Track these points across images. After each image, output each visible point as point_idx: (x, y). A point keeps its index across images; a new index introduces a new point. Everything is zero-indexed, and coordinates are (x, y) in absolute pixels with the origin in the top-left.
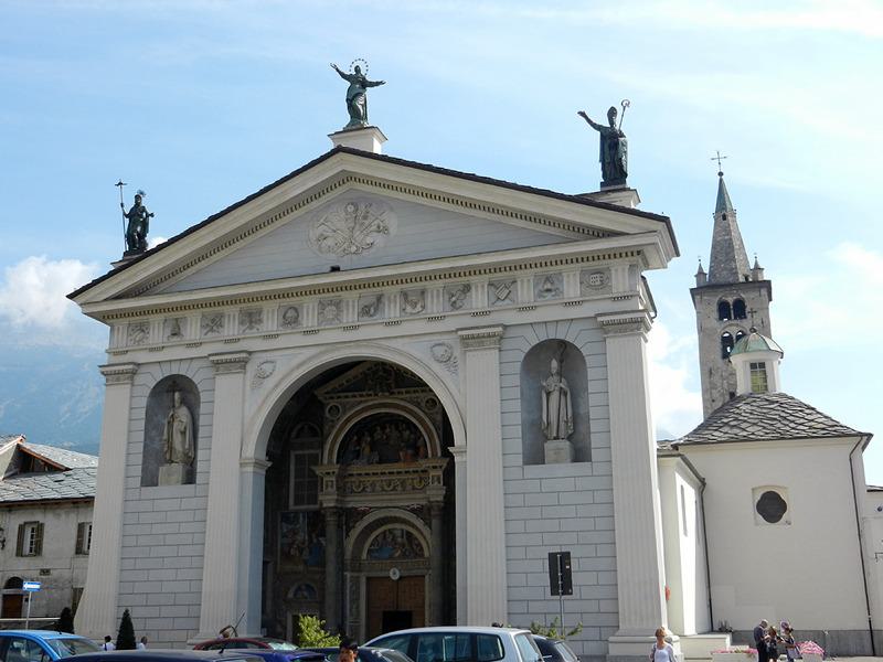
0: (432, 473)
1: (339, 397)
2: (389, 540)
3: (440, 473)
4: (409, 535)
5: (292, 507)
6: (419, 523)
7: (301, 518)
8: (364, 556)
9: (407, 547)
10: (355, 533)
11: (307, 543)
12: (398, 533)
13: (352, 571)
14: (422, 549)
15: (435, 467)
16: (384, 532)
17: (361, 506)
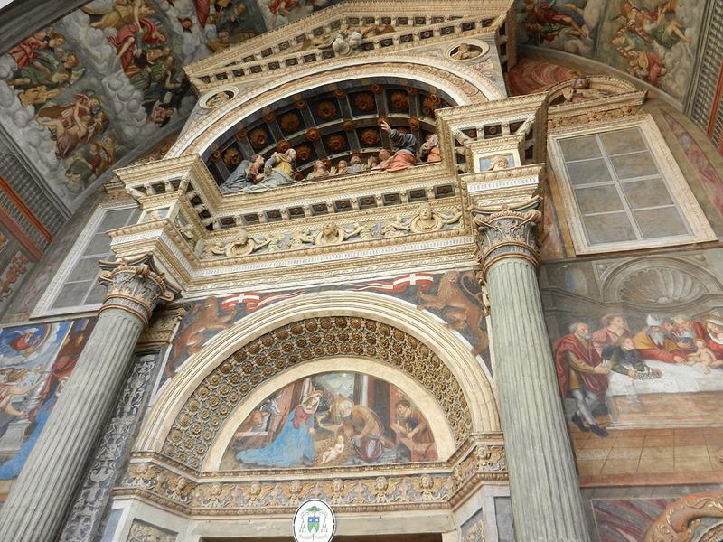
0: (482, 152)
1: (239, 73)
2: (309, 409)
3: (509, 147)
4: (381, 391)
5: (43, 307)
6: (425, 326)
7: (53, 338)
8: (214, 459)
9: (373, 428)
10: (194, 369)
11: (33, 404)
12: (343, 387)
13: (147, 497)
14: (426, 435)
15: (492, 131)
16: (300, 382)
17: (233, 293)
